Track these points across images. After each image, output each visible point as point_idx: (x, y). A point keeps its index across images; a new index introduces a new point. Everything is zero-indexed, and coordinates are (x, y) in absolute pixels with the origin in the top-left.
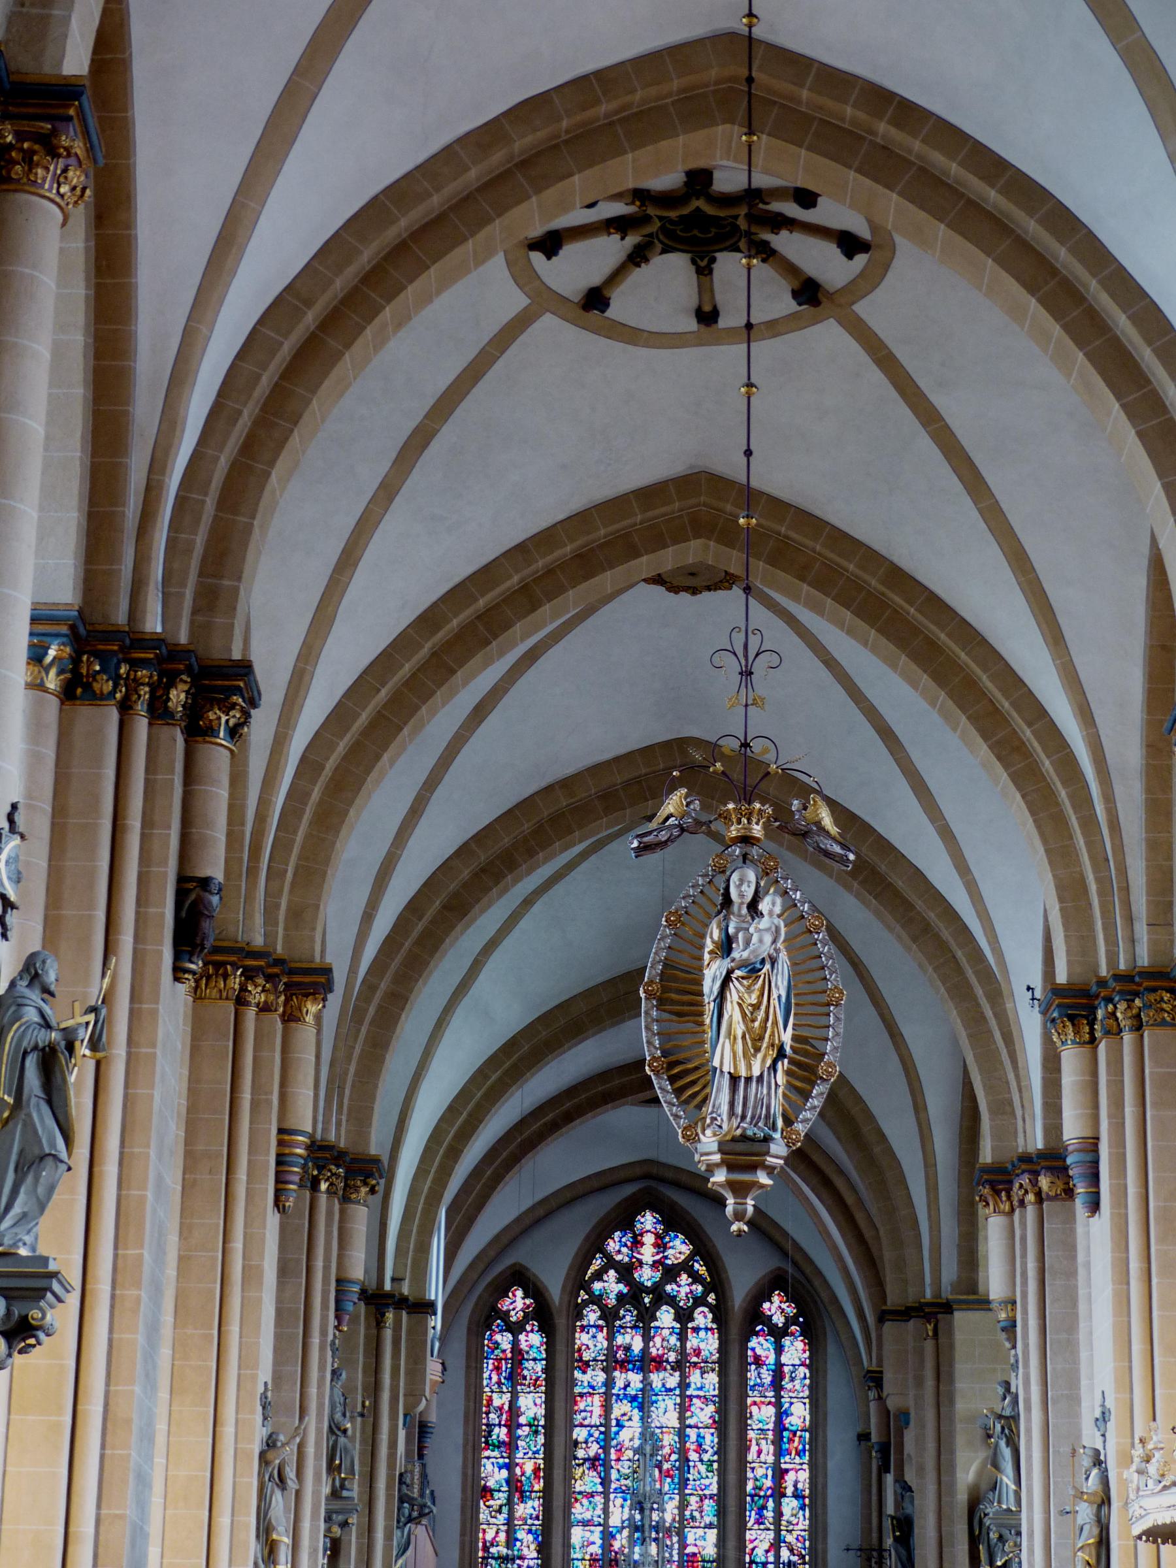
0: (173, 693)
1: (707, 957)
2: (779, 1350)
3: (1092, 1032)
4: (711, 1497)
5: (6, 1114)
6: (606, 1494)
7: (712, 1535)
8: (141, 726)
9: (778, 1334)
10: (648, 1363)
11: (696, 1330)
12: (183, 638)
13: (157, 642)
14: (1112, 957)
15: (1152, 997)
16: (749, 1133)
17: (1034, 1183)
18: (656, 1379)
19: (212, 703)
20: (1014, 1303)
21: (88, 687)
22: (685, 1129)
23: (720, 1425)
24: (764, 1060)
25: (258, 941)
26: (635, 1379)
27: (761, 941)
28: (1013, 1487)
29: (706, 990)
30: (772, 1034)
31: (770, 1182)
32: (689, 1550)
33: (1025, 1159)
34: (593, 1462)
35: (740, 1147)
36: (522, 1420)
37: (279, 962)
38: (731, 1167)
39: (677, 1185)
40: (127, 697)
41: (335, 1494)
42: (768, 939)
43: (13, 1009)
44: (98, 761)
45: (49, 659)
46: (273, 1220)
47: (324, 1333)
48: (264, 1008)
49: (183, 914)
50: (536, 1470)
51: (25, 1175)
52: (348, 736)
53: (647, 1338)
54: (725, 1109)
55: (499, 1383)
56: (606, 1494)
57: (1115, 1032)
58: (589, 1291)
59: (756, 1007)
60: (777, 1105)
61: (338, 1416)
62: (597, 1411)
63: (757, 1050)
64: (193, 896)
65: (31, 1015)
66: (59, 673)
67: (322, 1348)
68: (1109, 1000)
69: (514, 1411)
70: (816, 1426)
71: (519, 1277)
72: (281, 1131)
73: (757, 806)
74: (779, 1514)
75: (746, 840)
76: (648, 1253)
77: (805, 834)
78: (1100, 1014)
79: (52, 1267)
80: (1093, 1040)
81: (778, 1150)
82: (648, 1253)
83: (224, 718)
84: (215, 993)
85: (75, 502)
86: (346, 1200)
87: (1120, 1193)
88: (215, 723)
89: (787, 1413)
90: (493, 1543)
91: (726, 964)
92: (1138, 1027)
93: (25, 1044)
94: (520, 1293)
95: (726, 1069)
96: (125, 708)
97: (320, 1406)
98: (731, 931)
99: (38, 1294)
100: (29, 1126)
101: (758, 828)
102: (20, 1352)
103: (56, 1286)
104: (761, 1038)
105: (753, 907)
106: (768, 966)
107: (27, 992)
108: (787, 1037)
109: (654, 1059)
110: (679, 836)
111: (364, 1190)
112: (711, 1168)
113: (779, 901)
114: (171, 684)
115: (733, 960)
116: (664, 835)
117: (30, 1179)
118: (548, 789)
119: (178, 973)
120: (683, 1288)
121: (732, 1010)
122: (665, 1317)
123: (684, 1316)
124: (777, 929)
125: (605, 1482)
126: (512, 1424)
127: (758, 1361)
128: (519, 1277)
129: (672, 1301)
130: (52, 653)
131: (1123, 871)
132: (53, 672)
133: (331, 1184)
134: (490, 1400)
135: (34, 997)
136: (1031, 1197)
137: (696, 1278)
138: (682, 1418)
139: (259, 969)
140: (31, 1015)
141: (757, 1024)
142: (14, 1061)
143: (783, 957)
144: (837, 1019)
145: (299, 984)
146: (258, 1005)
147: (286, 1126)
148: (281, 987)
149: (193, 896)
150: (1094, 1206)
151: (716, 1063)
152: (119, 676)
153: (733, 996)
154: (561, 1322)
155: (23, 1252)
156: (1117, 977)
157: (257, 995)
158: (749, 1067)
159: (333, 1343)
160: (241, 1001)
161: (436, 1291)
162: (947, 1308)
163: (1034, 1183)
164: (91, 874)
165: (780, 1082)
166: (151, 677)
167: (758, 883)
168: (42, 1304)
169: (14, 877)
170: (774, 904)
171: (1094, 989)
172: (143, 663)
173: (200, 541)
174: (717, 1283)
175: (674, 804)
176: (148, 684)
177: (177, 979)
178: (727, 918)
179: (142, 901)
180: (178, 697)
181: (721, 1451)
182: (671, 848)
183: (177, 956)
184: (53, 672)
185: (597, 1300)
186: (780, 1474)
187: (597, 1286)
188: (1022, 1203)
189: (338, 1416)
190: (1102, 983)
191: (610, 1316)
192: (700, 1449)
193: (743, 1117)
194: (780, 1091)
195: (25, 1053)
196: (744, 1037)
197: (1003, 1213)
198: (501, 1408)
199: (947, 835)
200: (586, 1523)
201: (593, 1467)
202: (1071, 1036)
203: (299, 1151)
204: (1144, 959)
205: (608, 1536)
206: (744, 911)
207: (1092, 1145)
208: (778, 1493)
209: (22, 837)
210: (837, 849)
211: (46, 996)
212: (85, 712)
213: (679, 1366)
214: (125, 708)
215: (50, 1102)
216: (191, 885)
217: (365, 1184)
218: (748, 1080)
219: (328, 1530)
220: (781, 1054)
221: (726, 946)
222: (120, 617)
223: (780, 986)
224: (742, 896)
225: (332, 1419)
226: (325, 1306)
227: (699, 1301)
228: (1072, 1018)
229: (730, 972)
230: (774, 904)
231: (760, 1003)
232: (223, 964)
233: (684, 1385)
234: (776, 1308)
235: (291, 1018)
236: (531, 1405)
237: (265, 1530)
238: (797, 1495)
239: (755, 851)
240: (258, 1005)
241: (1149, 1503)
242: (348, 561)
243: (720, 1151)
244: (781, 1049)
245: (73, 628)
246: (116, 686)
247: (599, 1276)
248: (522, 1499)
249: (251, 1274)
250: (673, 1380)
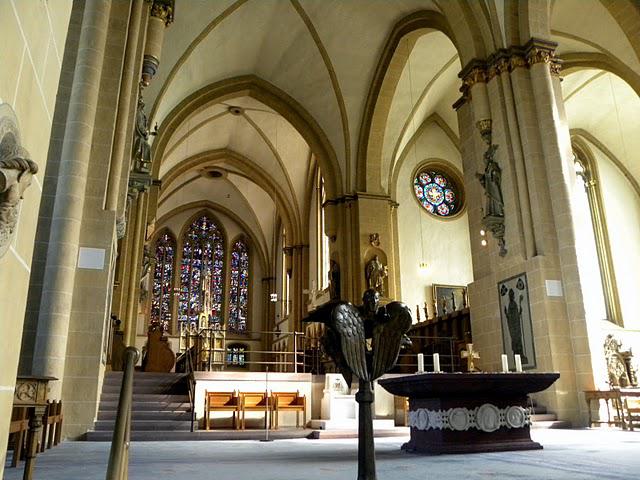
2: (240, 256)
9: (237, 250)
23: (223, 275)
39: (213, 209)
41: (136, 170)
61: (141, 124)
70: (250, 277)
71: (167, 231)
74: (238, 299)
76: (204, 228)
82: (204, 228)
127: (234, 258)
162: (355, 197)
181: (223, 281)
189: (141, 124)
192: (217, 282)
197: (483, 81)
208: (239, 294)
213: (211, 259)
219: (131, 191)
225: (137, 125)
238: (244, 295)
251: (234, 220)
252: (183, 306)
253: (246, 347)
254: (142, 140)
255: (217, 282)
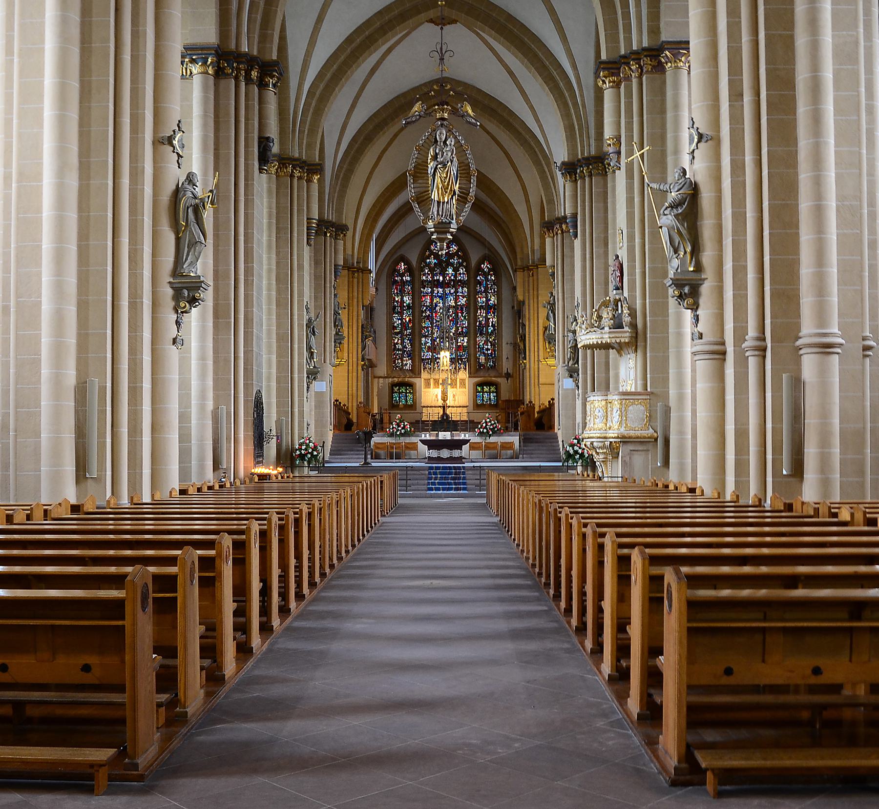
0: (253, 73)
1: (429, 161)
3: (576, 177)
4: (466, 327)
5: (183, 229)
6: (432, 327)
7: (466, 340)
8: (243, 85)
9: (485, 275)
10: (443, 285)
11: (460, 274)
12: (255, 53)
13: (246, 54)
14: (583, 153)
15: (595, 165)
16: (444, 221)
17: (561, 227)
18: (447, 291)
19: (267, 75)
20: (554, 266)
21: (223, 72)
22: (423, 220)
24: (448, 197)
25: (297, 155)
26: (441, 290)
27: (447, 154)
28: (553, 326)
29: (429, 172)
30: (451, 187)
31: (451, 237)
32: (459, 344)
33: (558, 219)
34: (428, 317)
35: (440, 226)
36: (405, 305)
37: (305, 162)
38: (438, 233)
40: (237, 75)
41: (337, 334)
42: (450, 154)
43: (183, 192)
44: (228, 99)
45: (209, 63)
46: (307, 249)
47: (331, 283)
48: (300, 178)
49: (261, 150)
50: (410, 320)
51: (191, 249)
52: (324, 82)
53: (444, 278)
54: (436, 213)
55: (397, 293)
56: (432, 327)
57: (583, 178)
58: (425, 262)
59: (446, 177)
60: (454, 211)
61: (337, 309)
62: (429, 301)
63: (446, 192)
64: (264, 143)
65: (189, 194)
66: (212, 68)
67: (330, 287)
68: (581, 166)
69: (402, 301)
71: (403, 259)
72: (307, 219)
73: (446, 107)
75: (443, 119)
77: (463, 116)
78: (578, 171)
79: (202, 279)
80: (576, 181)
81: (454, 227)
83: (271, 80)
84: (283, 174)
85: (214, 5)
86: (336, 239)
87: (584, 231)
88: (268, 83)
89: (490, 300)
90: (397, 343)
91: (436, 163)
92: (591, 176)
93: (187, 204)
94: (403, 264)
95: (436, 199)
96: (237, 78)
97: (331, 306)
98: (437, 151)
99: (198, 288)
100: (191, 232)
101: (446, 114)
102: (194, 307)
103: (203, 285)
104: (448, 189)
105: (445, 142)
106: (450, 163)
107: (187, 186)
108: (457, 188)
109: (412, 196)
110: (419, 119)
111: (342, 235)
112: (432, 233)
113: (453, 140)
114: (252, 70)
115: (438, 162)
116: (414, 119)
117: (192, 250)
118: (398, 97)
119: (261, 170)
120: (455, 261)
121: (438, 180)
122: (450, 271)
123: (456, 270)
124: (453, 150)
125: (432, 323)
126: (402, 306)
128: (403, 259)
129: (452, 265)
130: (210, 60)
131: (587, 122)
132: (210, 68)
133: (331, 234)
134: (395, 299)
135: (190, 188)
136: (560, 232)
137: (459, 257)
138: (456, 303)
139: (298, 165)
140: (189, 194)
141: (446, 183)
142: (184, 209)
143: (455, 159)
144: (474, 181)
145: (312, 169)
146: (297, 177)
147: (308, 217)
148: (305, 171)
149: (264, 143)
150: (576, 236)
151: (433, 197)
152: (233, 67)
153: (438, 175)
154: (416, 273)
155: (192, 274)
156: (583, 158)
157: (297, 174)
158: (444, 198)
159: (334, 285)
160: (292, 176)
161: (372, 265)
163: (561, 227)
164: (228, 138)
165: (454, 203)
166: (245, 67)
167: (446, 134)
168: (199, 291)
169: (181, 146)
170: (451, 141)
171: (576, 163)
172: (242, 63)
173: (259, 18)
174: (465, 258)
175: (417, 107)
176: (244, 70)
177: (260, 172)
178: (436, 147)
179: (246, 146)
180: (254, 74)
182: (417, 123)
183: (260, 165)
184: (210, 68)
185: (429, 265)
186: (487, 320)
187: (428, 261)
188: (557, 233)
189: (337, 309)
190: (579, 160)
191: (432, 270)
193: (442, 216)
194: (455, 206)
195: (188, 208)
196: (442, 188)
198: (397, 302)
199: (532, 108)
200: (426, 337)
201: (428, 319)
202: (569, 179)
203: (314, 225)
204: (593, 153)
205: (433, 341)
206: (442, 144)
207: (575, 216)
208: (487, 325)
209: (183, 132)
210: (473, 121)
211: (194, 187)
212: (223, 83)
213: (454, 286)
214: (237, 78)
215: (198, 224)
216: (262, 140)
217: (342, 233)
218: (443, 203)
220: (455, 193)
221: (435, 158)
222: (233, 46)
223: (454, 170)
224: (441, 139)
225: (334, 310)
226: (331, 274)
227: (461, 265)
228: (568, 173)
229: (437, 166)
230: (451, 141)
231: (447, 176)
232: (285, 164)
233: (456, 292)
234: (485, 266)
235: (309, 181)
236: (407, 300)
237: (309, 348)
238: (493, 326)
239: (445, 123)
240: (297, 177)
241: (583, 338)
242: (320, 20)
243: (434, 228)
244: (454, 191)
245: (216, 51)
246: (233, 71)
247: (429, 258)
248: (406, 330)
249: (301, 267)
250: (452, 291)
251: (475, 237)
252: (426, 343)
253: (496, 385)
254: (338, 316)
255: (462, 313)
